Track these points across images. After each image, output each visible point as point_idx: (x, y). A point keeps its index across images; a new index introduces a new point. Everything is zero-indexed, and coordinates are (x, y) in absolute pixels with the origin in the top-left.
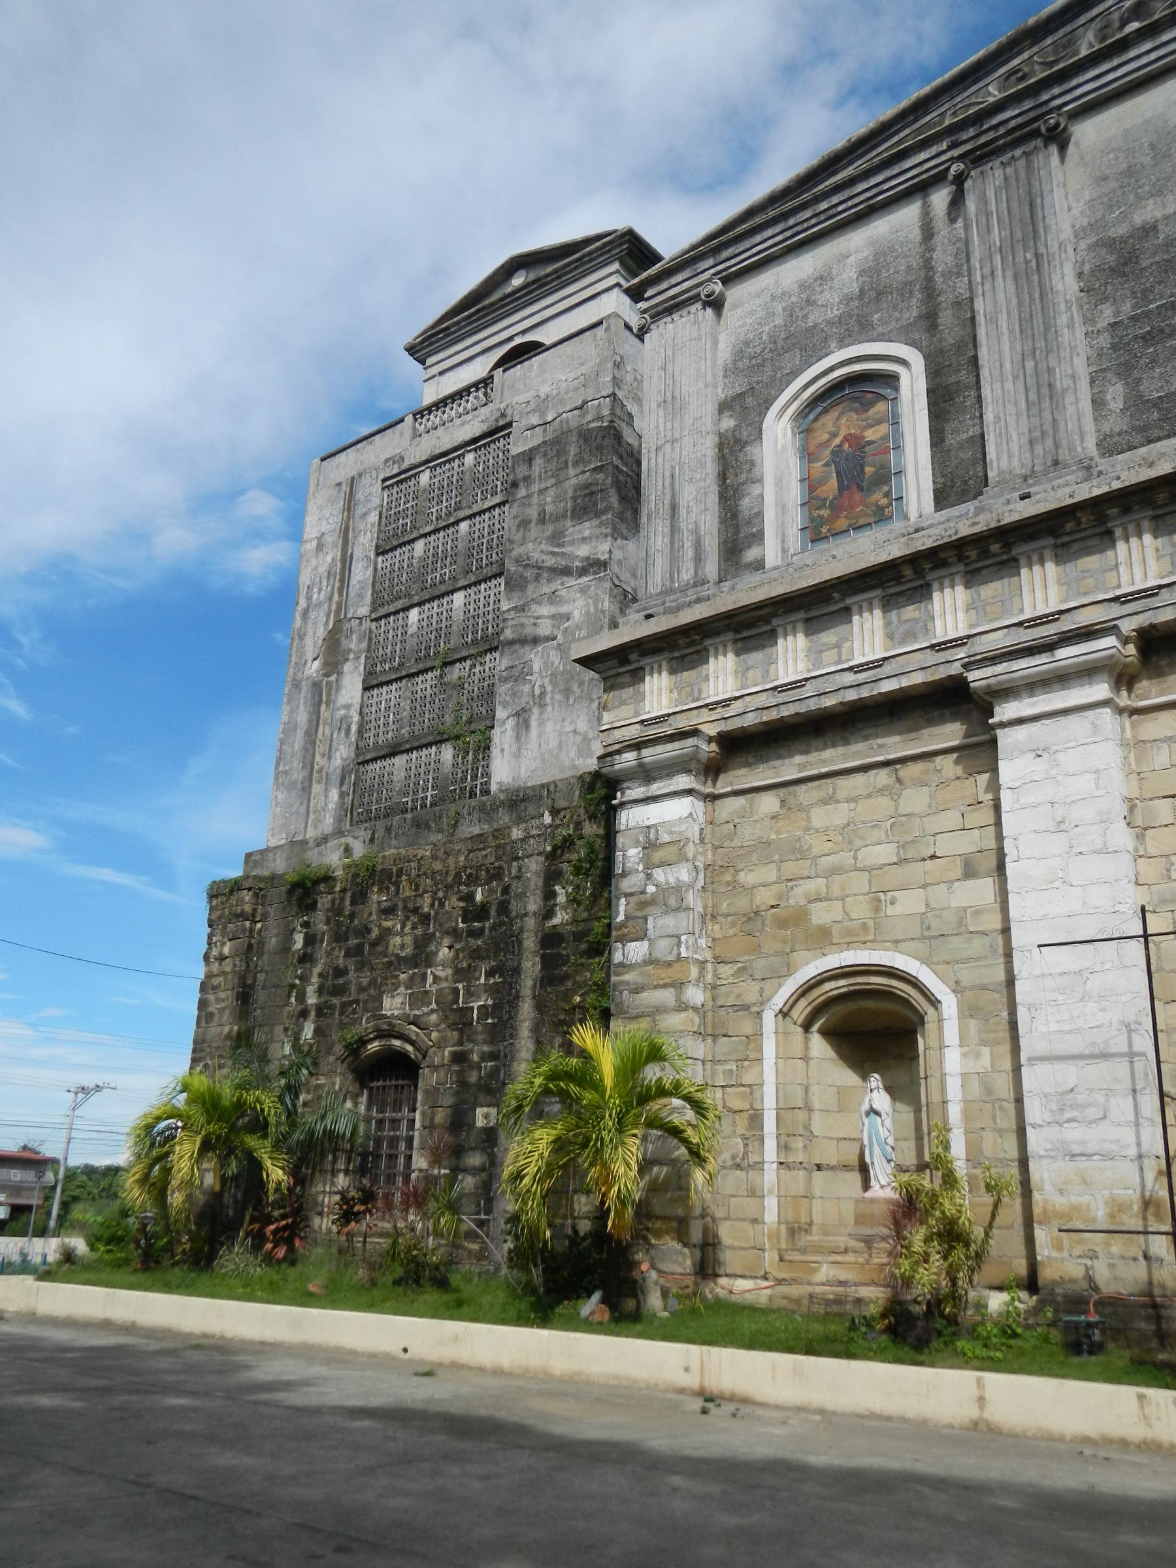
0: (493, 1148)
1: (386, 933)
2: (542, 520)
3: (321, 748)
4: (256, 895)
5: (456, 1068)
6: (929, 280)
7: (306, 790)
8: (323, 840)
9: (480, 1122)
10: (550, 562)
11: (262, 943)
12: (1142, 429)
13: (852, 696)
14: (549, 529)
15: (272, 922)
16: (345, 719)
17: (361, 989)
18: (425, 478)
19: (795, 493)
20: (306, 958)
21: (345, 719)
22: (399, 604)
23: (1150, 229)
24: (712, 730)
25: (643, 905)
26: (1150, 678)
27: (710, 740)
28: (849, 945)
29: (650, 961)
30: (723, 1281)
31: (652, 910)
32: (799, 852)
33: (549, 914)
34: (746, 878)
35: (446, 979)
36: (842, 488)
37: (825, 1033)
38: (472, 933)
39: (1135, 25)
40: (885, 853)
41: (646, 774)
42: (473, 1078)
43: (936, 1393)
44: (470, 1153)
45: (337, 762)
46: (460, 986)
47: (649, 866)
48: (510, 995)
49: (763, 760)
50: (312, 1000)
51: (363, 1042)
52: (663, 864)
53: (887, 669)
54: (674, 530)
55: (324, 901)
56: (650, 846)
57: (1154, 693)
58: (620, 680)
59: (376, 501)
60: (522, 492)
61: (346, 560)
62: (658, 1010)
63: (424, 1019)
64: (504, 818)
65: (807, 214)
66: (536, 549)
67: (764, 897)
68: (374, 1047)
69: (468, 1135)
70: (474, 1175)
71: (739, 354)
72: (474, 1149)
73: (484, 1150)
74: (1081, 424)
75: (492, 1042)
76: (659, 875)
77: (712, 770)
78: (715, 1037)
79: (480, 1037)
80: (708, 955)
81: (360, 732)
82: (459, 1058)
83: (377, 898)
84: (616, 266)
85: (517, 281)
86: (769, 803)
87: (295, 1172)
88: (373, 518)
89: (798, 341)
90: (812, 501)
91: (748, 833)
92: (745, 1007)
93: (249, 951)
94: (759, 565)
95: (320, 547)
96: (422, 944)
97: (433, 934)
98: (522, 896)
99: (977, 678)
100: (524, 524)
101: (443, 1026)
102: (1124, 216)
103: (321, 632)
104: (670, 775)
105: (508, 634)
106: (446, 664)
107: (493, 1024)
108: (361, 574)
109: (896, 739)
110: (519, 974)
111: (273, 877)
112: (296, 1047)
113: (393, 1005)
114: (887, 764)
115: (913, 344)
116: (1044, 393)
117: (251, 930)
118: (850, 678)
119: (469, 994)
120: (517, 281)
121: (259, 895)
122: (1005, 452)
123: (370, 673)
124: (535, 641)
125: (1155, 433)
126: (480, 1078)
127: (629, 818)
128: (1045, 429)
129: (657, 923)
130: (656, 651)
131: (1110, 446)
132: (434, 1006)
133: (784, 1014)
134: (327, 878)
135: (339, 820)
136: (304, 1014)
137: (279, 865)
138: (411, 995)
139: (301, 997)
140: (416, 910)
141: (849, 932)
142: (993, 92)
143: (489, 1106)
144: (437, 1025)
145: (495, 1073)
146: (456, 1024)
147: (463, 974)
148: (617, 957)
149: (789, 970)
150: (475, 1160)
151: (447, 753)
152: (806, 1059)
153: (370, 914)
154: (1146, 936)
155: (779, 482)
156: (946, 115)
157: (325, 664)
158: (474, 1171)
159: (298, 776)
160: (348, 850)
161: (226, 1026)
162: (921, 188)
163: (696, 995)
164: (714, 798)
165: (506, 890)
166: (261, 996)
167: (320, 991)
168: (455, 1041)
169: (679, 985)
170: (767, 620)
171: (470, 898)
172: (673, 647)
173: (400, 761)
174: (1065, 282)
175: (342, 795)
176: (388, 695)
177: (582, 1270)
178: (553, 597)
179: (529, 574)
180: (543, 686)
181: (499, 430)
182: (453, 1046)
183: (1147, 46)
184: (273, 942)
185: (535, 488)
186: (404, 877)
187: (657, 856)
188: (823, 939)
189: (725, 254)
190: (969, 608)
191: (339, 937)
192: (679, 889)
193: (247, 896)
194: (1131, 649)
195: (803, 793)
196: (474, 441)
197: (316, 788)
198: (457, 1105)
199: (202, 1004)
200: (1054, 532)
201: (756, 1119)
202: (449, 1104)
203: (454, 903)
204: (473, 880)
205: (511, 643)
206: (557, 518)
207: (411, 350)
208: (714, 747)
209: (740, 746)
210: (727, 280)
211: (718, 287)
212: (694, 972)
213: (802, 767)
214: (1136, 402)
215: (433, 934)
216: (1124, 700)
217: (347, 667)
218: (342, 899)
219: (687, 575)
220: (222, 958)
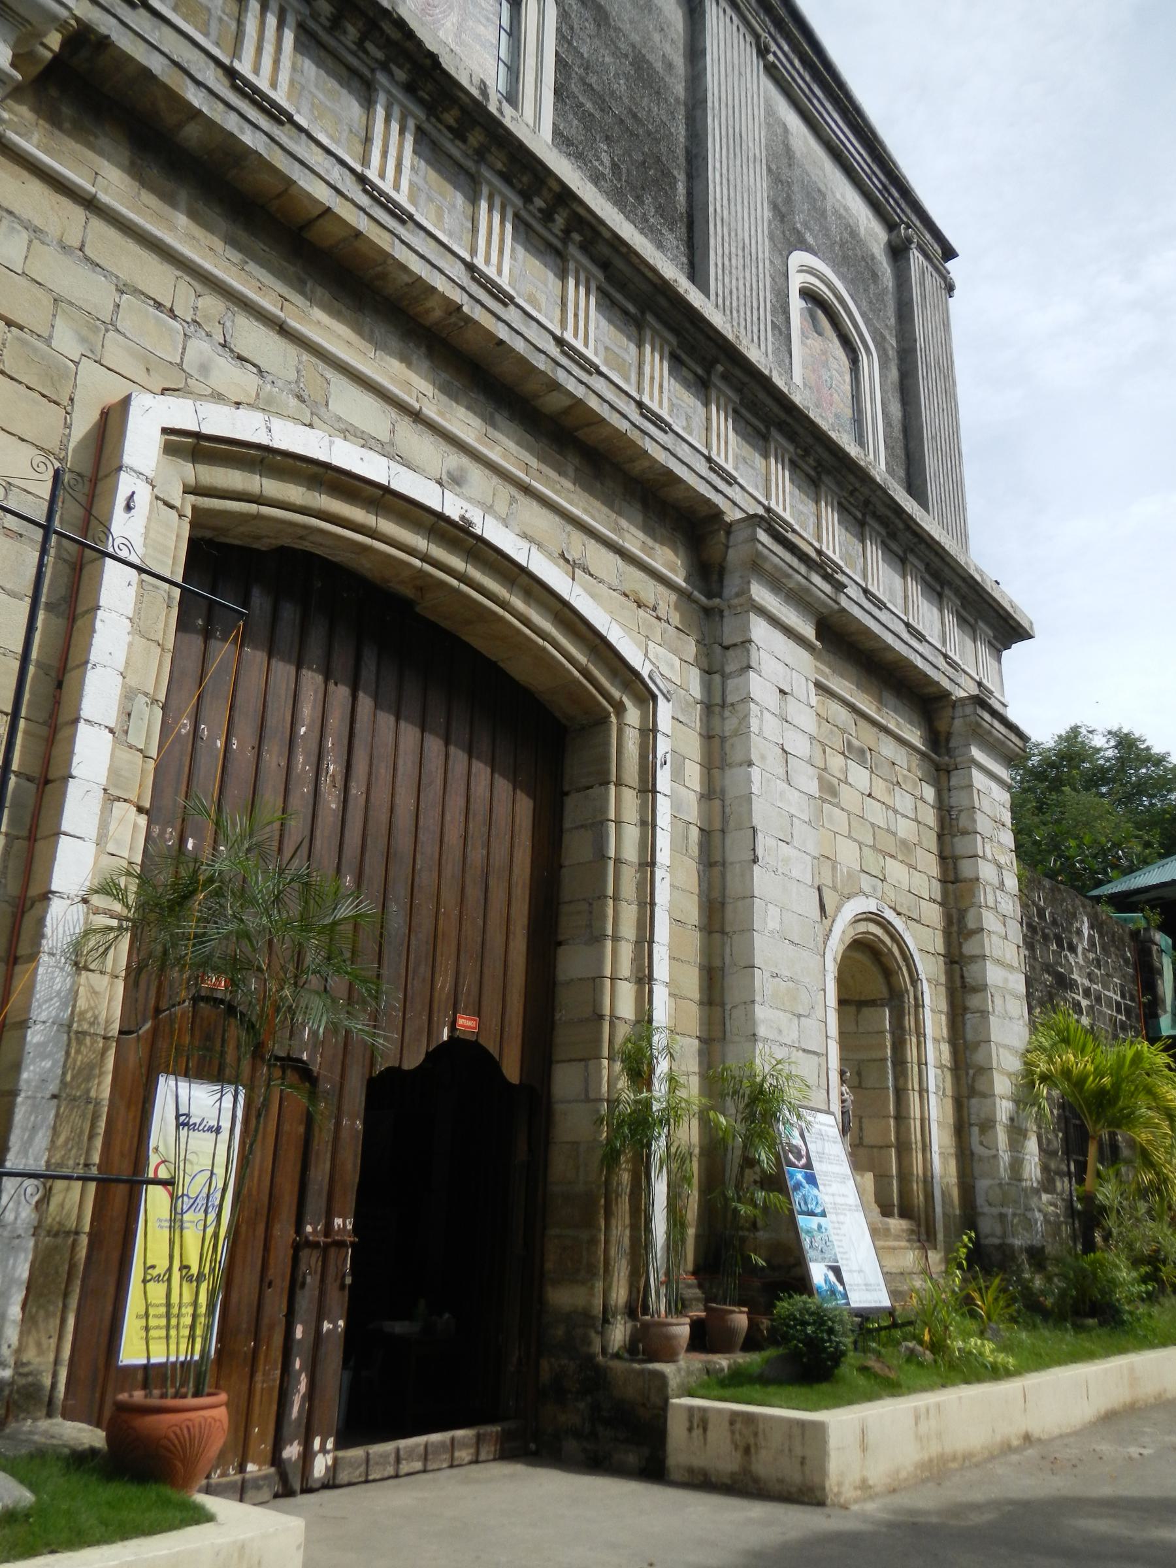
26: (36, 110)
57: (36, 137)
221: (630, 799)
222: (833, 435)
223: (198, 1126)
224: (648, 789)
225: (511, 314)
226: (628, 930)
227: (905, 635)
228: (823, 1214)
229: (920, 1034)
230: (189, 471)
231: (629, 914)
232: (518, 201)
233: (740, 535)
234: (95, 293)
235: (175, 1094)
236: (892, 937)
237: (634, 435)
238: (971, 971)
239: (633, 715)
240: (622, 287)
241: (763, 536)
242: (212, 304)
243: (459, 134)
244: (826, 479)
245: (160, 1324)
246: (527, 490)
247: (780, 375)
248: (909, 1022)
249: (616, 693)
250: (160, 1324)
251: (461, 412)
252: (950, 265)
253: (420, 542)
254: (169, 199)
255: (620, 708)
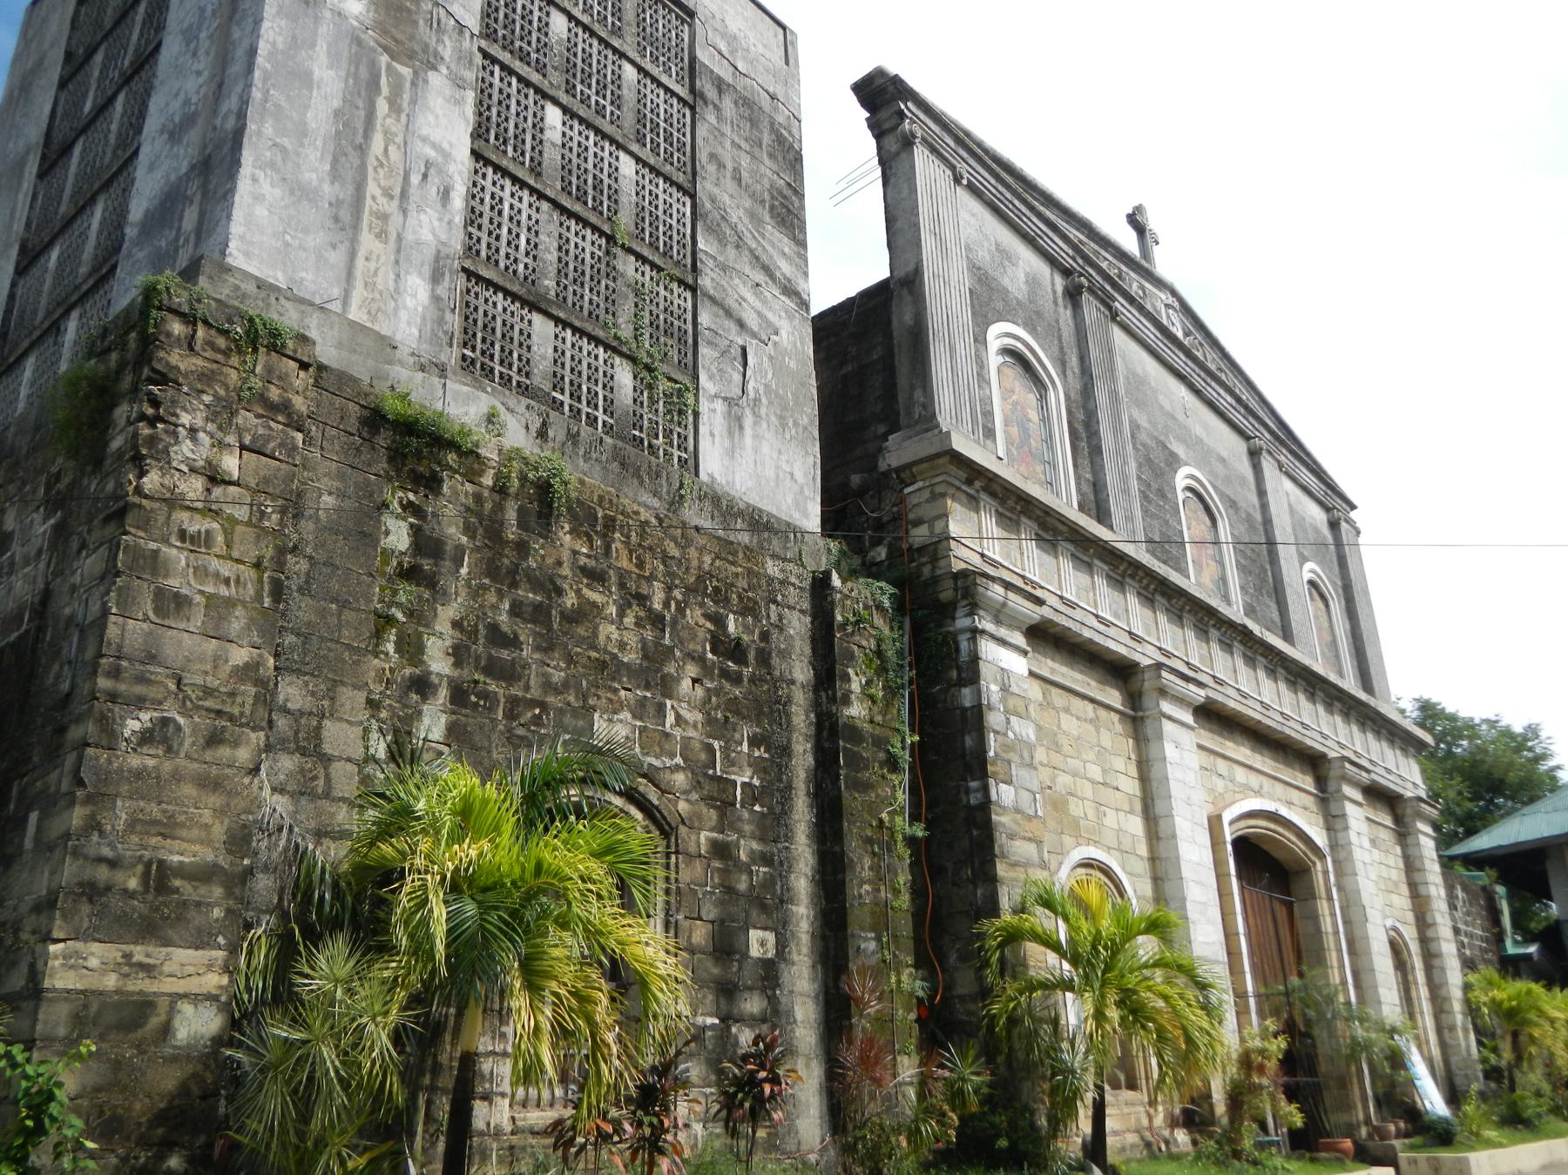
0: (774, 990)
5: (717, 864)
9: (755, 951)
17: (548, 686)
35: (695, 726)
42: (742, 886)
44: (747, 995)
46: (716, 745)
48: (780, 780)
58: (958, 494)
63: (667, 775)
69: (740, 968)
70: (751, 1027)
72: (750, 989)
73: (763, 990)
75: (762, 840)
79: (747, 828)
82: (721, 850)
97: (670, 650)
98: (785, 655)
101: (695, 796)
107: (762, 813)
110: (790, 756)
126: (752, 887)
132: (679, 760)
136: (422, 686)
138: (643, 730)
139: (412, 649)
140: (642, 599)
143: (765, 928)
144: (685, 792)
145: (768, 883)
146: (712, 798)
147: (719, 727)
150: (753, 1004)
153: (559, 563)
156: (1090, 247)
158: (752, 1021)
165: (765, 636)
168: (713, 823)
180: (757, 391)
182: (712, 830)
186: (617, 535)
198: (722, 921)
202: (711, 917)
215: (670, 650)
218: (499, 508)
221: (1325, 904)
224: (1330, 898)
226: (1335, 964)
229: (1416, 983)
231: (1334, 954)
233: (1336, 765)
238: (1433, 946)
239: (1319, 866)
241: (1347, 765)
248: (1410, 978)
252: (1353, 515)
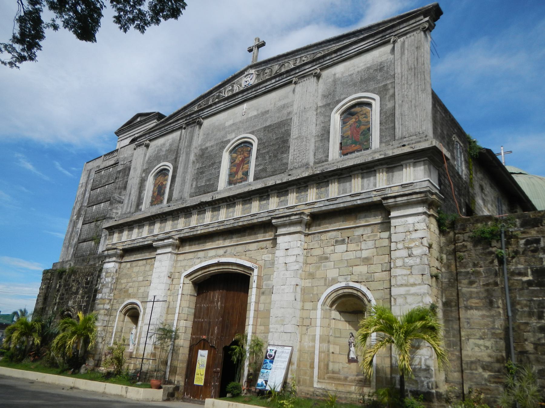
1: (73, 286)
2: (119, 189)
3: (72, 238)
4: (52, 274)
6: (178, 150)
7: (68, 248)
8: (67, 262)
10: (118, 199)
11: (51, 286)
12: (196, 193)
13: (141, 244)
14: (119, 191)
15: (54, 281)
16: (78, 231)
17: (66, 299)
18: (103, 172)
19: (151, 194)
20: (58, 291)
21: (78, 231)
22: (92, 204)
23: (207, 148)
24: (121, 248)
25: (103, 286)
27: (121, 250)
28: (132, 298)
29: (101, 298)
30: (100, 368)
31: (104, 287)
32: (130, 277)
33: (96, 285)
34: (122, 281)
36: (158, 194)
37: (129, 316)
38: (86, 288)
39: (217, 100)
40: (141, 279)
41: (110, 256)
43: (113, 389)
45: (74, 242)
47: (106, 277)
49: (130, 255)
50: (57, 301)
51: (64, 312)
52: (108, 277)
53: (146, 239)
54: (129, 199)
55: (64, 277)
56: (107, 273)
59: (93, 177)
60: (117, 181)
61: (86, 190)
62: (100, 309)
64: (97, 261)
65: (163, 129)
66: (116, 195)
67: (123, 286)
68: (66, 313)
71: (149, 159)
74: (188, 189)
76: (106, 279)
77: (122, 256)
78: (110, 316)
80: (112, 298)
81: (80, 235)
83: (73, 277)
84: (156, 121)
85: (138, 120)
86: (129, 265)
87: (42, 342)
88: (92, 181)
89: (157, 158)
90: (153, 197)
91: (125, 271)
92: (116, 310)
93: (48, 288)
94: (141, 210)
95: (82, 186)
96: (78, 289)
99: (155, 244)
100: (116, 189)
102: (205, 144)
103: (78, 208)
104: (113, 257)
105: (108, 216)
106: (97, 221)
108: (87, 195)
109: (147, 254)
111: (56, 270)
112: (53, 312)
113: (70, 303)
114: (146, 259)
115: (172, 164)
116: (184, 182)
117: (49, 283)
118: (141, 240)
119: (83, 302)
120: (138, 120)
121: (52, 274)
122: (175, 195)
123: (84, 221)
124: (112, 218)
125: (197, 194)
127: (106, 266)
128: (181, 191)
129: (106, 290)
130: (116, 228)
131: (191, 196)
133: (121, 311)
134: (65, 271)
135: (72, 257)
136: (55, 304)
137: (58, 267)
139: (56, 300)
140: (78, 281)
141: (133, 295)
142: (196, 109)
147: (83, 297)
148: (97, 297)
149: (124, 302)
151: (93, 243)
152: (123, 321)
154: (154, 302)
155: (148, 191)
157: (77, 217)
159: (67, 244)
160: (70, 265)
161: (40, 306)
162: (181, 128)
163: (108, 307)
164: (121, 263)
166: (49, 299)
167: (59, 299)
169: (104, 304)
170: (132, 225)
171: (87, 279)
172: (119, 228)
173: (85, 243)
174: (192, 157)
175: (74, 250)
176: (86, 226)
177: (74, 364)
178: (117, 208)
179: (114, 201)
181: (116, 164)
183: (214, 107)
184: (54, 286)
185: (120, 180)
187: (108, 275)
188: (129, 296)
189: (151, 134)
190: (160, 228)
191: (65, 286)
192: (108, 283)
193: (49, 274)
194: (177, 241)
195: (134, 264)
196: (112, 165)
197: (70, 248)
199: (37, 300)
200: (172, 215)
201: (112, 334)
203: (84, 280)
204: (88, 275)
205: (108, 218)
206: (121, 189)
207: (116, 133)
208: (121, 251)
209: (127, 251)
210: (150, 140)
211: (148, 142)
212: (108, 301)
213: (135, 258)
214: (197, 187)
216: (176, 251)
217: (80, 218)
219: (128, 210)
220: (42, 289)
222: (298, 177)
223: (203, 356)
225: (225, 223)
227: (352, 199)
228: (271, 369)
230: (189, 278)
232: (225, 204)
234: (184, 263)
235: (201, 352)
236: (357, 291)
237: (250, 222)
240: (246, 197)
242: (196, 253)
243: (216, 204)
244: (308, 184)
245: (199, 379)
246: (237, 245)
247: (279, 180)
249: (249, 272)
250: (199, 379)
251: (226, 241)
253: (216, 268)
254: (192, 245)
255: (251, 274)
